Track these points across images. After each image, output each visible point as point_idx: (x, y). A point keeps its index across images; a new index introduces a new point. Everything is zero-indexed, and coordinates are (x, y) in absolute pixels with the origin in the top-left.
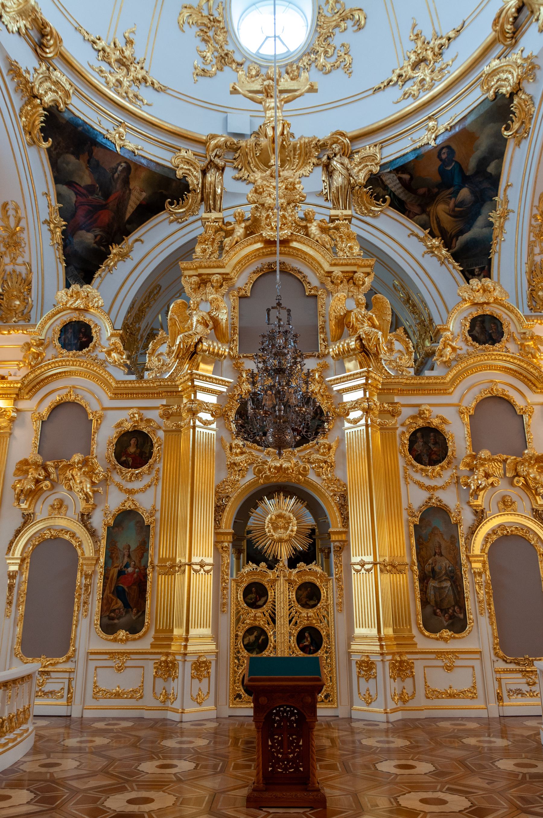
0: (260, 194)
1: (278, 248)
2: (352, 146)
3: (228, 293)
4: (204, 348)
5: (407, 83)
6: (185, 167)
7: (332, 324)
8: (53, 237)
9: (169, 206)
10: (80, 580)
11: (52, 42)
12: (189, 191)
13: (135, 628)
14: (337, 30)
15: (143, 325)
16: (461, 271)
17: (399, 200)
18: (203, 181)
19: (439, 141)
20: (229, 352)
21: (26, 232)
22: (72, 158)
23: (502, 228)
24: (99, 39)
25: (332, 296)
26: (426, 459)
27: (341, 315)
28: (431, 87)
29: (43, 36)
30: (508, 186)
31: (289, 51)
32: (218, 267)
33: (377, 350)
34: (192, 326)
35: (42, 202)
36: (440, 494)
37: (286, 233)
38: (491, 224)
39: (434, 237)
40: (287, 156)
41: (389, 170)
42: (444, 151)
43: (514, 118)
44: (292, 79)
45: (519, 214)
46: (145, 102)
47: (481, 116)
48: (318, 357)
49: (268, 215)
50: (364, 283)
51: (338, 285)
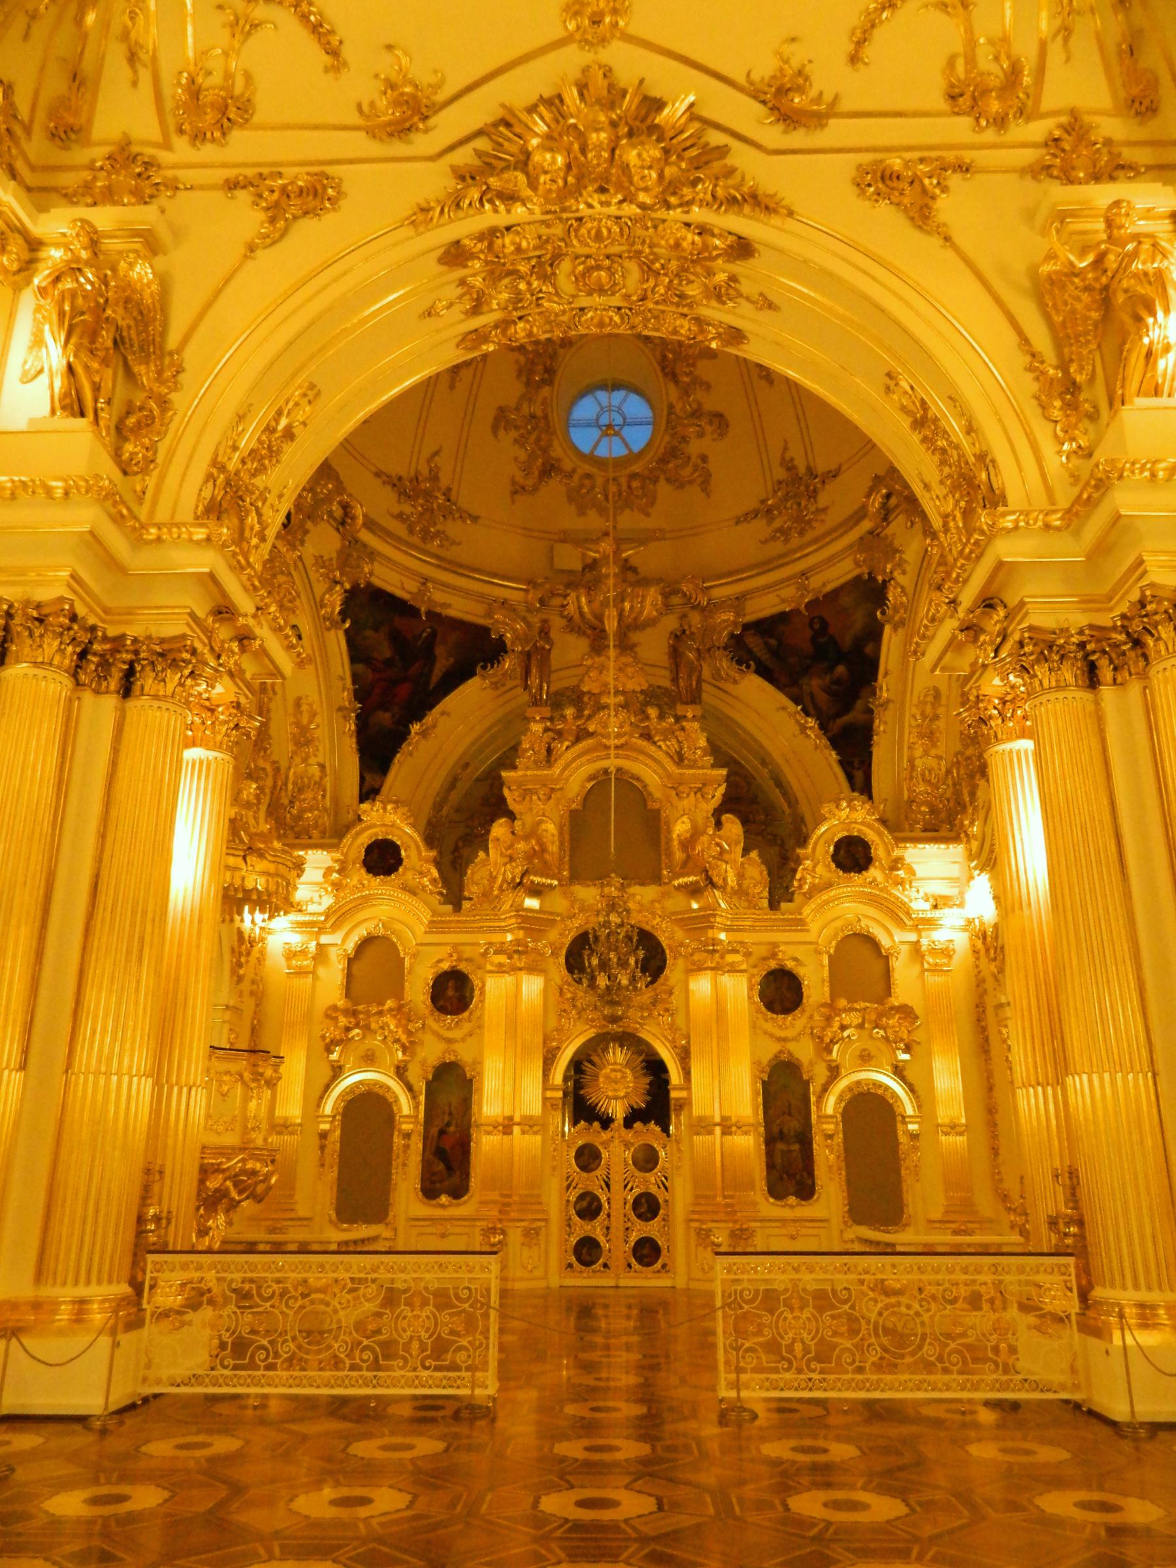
10: (397, 1140)
13: (459, 1192)
26: (777, 1006)
30: (886, 674)
31: (630, 451)
36: (791, 1046)
38: (871, 712)
39: (807, 714)
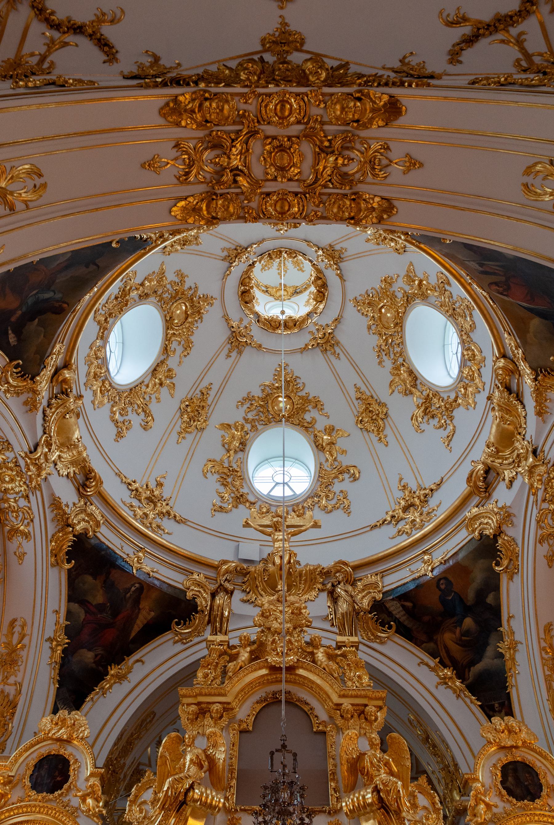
0: (267, 617)
1: (284, 675)
2: (354, 574)
3: (228, 726)
4: (196, 796)
5: (400, 523)
6: (196, 589)
7: (343, 770)
8: (52, 656)
9: (175, 626)
11: (94, 484)
12: (197, 612)
14: (336, 480)
15: (128, 761)
16: (480, 706)
17: (405, 627)
18: (211, 604)
19: (436, 572)
20: (224, 804)
21: (26, 650)
22: (89, 579)
23: (513, 659)
24: (134, 482)
25: (343, 733)
27: (353, 758)
28: (422, 527)
29: (87, 479)
30: (510, 617)
31: (295, 494)
32: (220, 695)
33: (398, 806)
34: (185, 767)
35: (51, 619)
37: (292, 658)
38: (501, 656)
39: (445, 666)
40: (293, 582)
41: (391, 597)
42: (442, 582)
43: (502, 556)
44: (298, 516)
45: (527, 646)
46: (166, 531)
47: (471, 552)
48: (329, 813)
49: (274, 640)
50: (376, 719)
51: (348, 720)
